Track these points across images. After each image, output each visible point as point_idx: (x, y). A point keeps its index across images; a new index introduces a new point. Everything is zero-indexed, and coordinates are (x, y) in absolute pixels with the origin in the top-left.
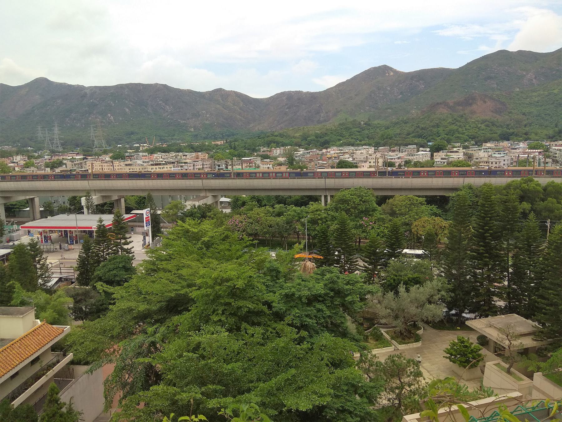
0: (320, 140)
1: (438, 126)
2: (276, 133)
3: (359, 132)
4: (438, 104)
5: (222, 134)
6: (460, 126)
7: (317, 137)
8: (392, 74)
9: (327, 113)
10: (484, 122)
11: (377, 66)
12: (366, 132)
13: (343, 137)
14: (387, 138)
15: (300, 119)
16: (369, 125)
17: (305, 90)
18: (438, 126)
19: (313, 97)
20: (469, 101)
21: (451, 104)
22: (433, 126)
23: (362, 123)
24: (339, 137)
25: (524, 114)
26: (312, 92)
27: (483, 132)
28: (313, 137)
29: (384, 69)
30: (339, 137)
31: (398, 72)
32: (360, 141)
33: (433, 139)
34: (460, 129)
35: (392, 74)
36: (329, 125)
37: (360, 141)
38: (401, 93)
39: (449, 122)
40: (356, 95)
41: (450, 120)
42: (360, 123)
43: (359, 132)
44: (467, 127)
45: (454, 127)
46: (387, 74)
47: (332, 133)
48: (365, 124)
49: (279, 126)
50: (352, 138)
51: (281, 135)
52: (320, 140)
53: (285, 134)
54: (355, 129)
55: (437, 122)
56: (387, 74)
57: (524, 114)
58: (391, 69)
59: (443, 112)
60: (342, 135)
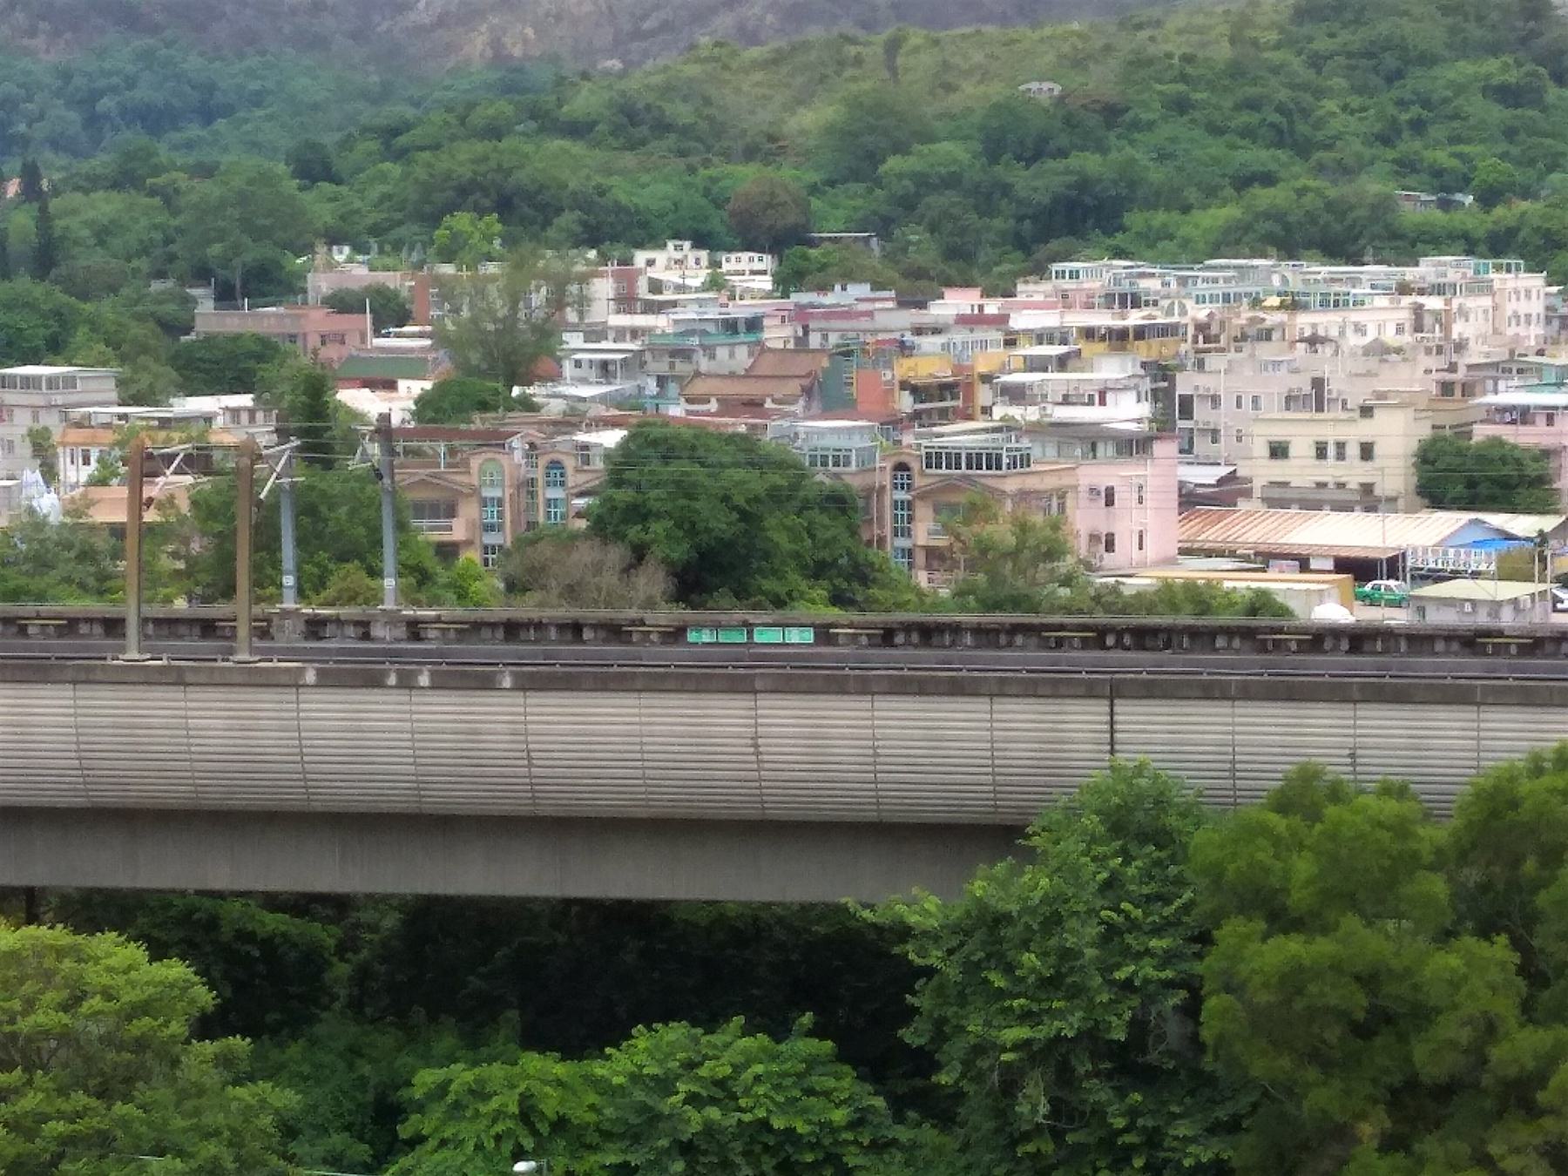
2: (584, 102)
3: (1507, 95)
5: (87, 102)
7: (994, 147)
13: (1303, 149)
24: (1257, 156)
28: (953, 152)
30: (1257, 156)
32: (1489, 198)
37: (1489, 198)
43: (1507, 95)
47: (1181, 106)
51: (634, 124)
53: (682, 112)
54: (1464, 69)
60: (1292, 134)
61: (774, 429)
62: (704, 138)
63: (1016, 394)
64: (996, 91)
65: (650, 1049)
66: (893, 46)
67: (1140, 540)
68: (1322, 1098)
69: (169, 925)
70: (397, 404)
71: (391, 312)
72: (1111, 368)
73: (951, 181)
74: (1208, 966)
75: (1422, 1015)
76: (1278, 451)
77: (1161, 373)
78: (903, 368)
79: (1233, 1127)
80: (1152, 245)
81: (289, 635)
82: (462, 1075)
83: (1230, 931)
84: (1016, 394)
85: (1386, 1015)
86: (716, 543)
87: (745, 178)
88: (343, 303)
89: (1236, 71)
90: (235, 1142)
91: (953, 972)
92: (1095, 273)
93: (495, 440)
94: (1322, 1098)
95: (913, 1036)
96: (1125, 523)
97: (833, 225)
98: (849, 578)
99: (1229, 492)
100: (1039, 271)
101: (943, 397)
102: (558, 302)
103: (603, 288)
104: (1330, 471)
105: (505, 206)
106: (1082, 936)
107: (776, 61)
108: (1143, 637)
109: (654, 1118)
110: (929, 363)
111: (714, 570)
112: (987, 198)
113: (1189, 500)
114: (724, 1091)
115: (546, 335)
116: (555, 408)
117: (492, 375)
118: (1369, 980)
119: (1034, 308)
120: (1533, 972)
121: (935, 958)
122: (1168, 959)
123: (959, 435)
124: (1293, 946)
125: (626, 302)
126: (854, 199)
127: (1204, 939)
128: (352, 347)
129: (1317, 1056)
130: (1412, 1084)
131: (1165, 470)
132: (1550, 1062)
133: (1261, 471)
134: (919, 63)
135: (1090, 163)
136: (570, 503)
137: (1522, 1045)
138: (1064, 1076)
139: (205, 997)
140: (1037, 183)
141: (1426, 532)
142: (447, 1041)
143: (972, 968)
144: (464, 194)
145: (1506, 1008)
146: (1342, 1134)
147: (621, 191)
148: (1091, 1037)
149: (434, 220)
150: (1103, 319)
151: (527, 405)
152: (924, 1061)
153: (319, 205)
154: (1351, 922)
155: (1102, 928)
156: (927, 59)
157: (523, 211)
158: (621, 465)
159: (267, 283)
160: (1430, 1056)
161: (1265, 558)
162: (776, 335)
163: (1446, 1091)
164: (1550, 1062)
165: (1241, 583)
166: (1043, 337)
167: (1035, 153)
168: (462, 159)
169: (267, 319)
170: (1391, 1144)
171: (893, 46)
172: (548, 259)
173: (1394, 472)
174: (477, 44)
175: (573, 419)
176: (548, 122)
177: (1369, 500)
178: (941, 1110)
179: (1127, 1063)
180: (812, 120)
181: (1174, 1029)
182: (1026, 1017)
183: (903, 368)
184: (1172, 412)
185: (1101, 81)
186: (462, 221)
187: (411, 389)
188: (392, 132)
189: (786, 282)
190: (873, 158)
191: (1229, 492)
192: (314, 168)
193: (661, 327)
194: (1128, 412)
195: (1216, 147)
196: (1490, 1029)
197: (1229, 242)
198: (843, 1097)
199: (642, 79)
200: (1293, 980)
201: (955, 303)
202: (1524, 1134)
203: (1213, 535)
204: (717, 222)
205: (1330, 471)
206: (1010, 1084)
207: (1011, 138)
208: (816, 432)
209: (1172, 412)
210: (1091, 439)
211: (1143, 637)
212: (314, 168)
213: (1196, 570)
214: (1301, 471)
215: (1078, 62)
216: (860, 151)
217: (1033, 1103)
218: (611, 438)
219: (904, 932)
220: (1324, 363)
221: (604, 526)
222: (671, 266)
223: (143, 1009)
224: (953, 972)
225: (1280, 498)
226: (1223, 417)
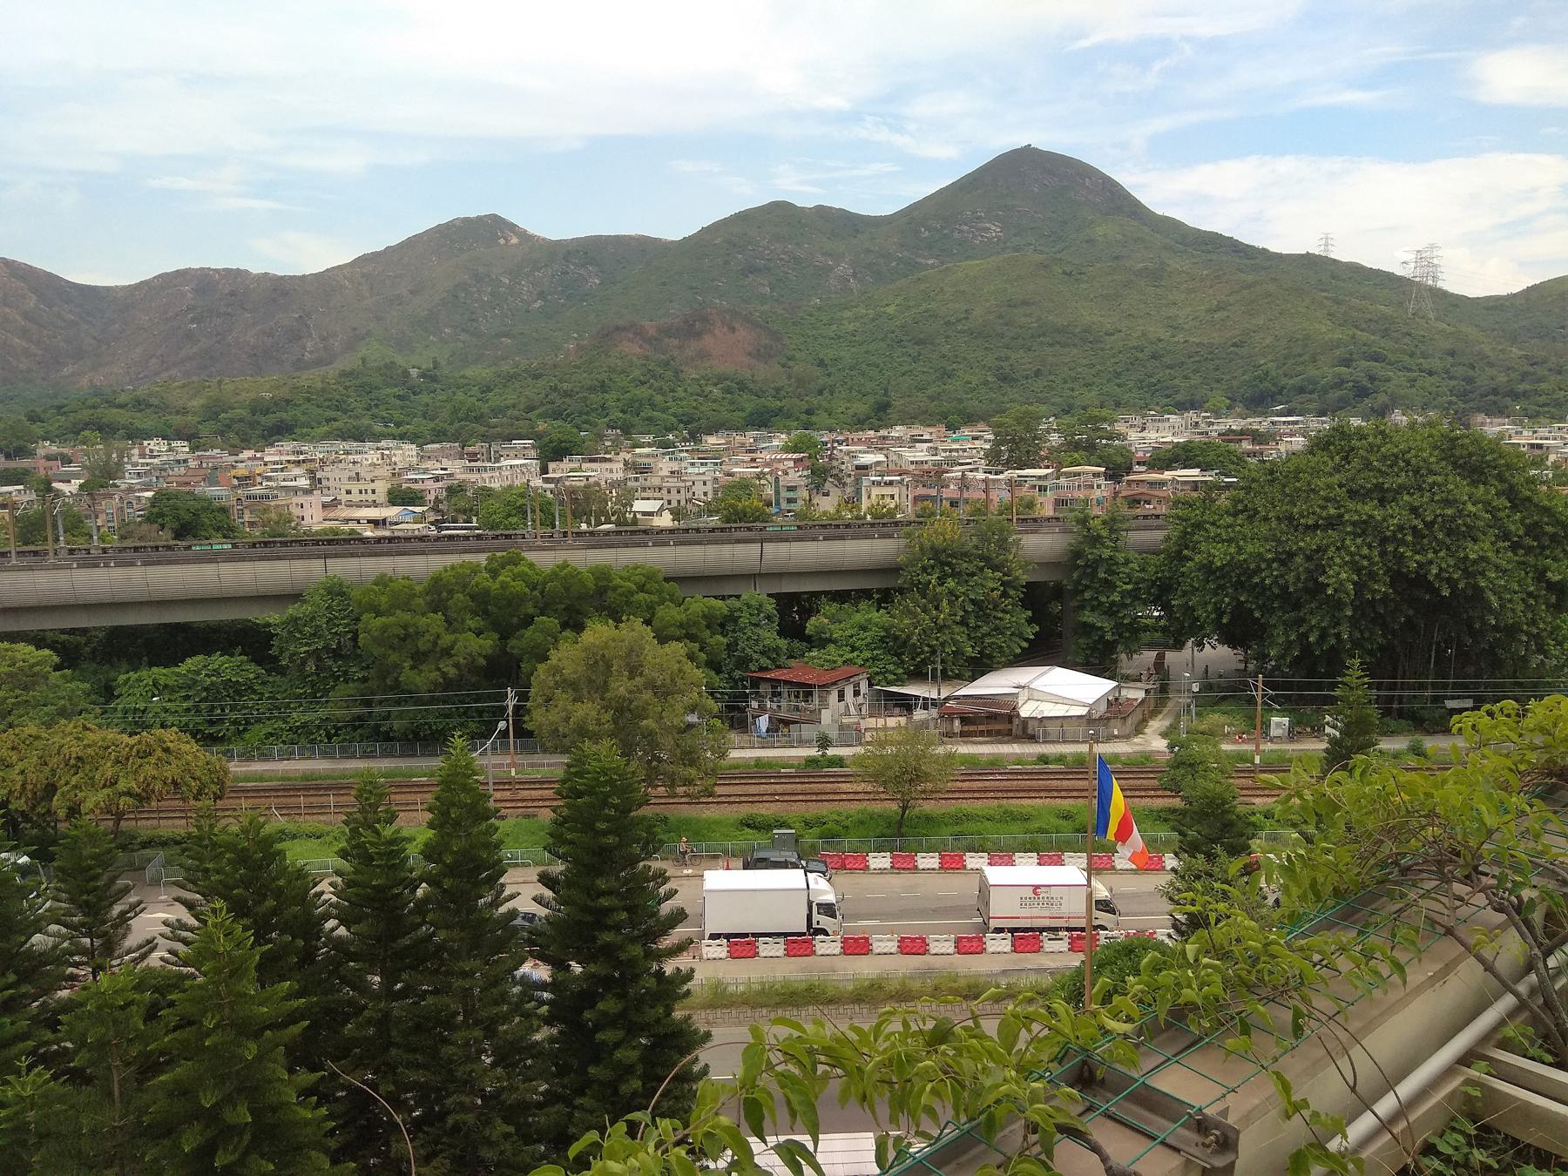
0: (263, 420)
1: (603, 387)
2: (122, 399)
4: (617, 328)
6: (660, 391)
8: (514, 240)
9: (323, 339)
10: (720, 379)
11: (473, 215)
12: (425, 398)
14: (466, 418)
15: (252, 354)
16: (434, 379)
17: (256, 268)
18: (603, 387)
19: (280, 290)
20: (693, 327)
21: (652, 332)
22: (592, 389)
23: (414, 372)
24: (330, 413)
25: (821, 363)
26: (280, 273)
27: (715, 406)
29: (492, 228)
30: (330, 413)
31: (533, 237)
33: (586, 422)
34: (659, 398)
35: (514, 240)
36: (311, 378)
38: (541, 295)
39: (634, 380)
40: (412, 292)
41: (637, 373)
42: (406, 374)
44: (680, 392)
45: (642, 392)
46: (502, 241)
47: (309, 400)
48: (423, 375)
49: (165, 375)
50: (374, 416)
51: (140, 404)
52: (263, 420)
53: (153, 401)
55: (604, 376)
56: (502, 241)
57: (821, 363)
58: (512, 227)
59: (631, 349)
61: (198, 490)
62: (162, 408)
63: (269, 479)
64: (253, 395)
66: (219, 382)
67: (313, 517)
69: (39, 641)
70: (72, 487)
71: (67, 460)
72: (297, 471)
73: (241, 420)
76: (348, 492)
77: (312, 472)
78: (233, 472)
79: (368, 667)
80: (303, 438)
81: (63, 554)
84: (269, 479)
86: (184, 523)
87: (177, 420)
88: (48, 458)
89: (323, 390)
91: (285, 634)
92: (288, 446)
93: (111, 496)
95: (274, 652)
96: (307, 513)
97: (205, 430)
98: (228, 531)
99: (335, 503)
100: (272, 445)
101: (246, 480)
102: (121, 457)
103: (136, 451)
104: (363, 497)
105: (100, 429)
107: (184, 386)
108: (316, 542)
110: (242, 470)
111: (186, 530)
112: (253, 425)
113: (324, 506)
115: (120, 464)
116: (123, 487)
117: (101, 479)
119: (271, 455)
121: (279, 631)
123: (256, 490)
125: (142, 456)
126: (211, 426)
128: (55, 470)
131: (318, 498)
133: (344, 497)
134: (228, 387)
135: (284, 415)
136: (135, 514)
138: (319, 659)
139: (56, 659)
140: (268, 420)
141: (392, 512)
143: (290, 632)
144: (86, 426)
147: (137, 423)
148: (326, 648)
149: (78, 433)
150: (292, 458)
151: (115, 485)
153: (37, 429)
156: (231, 387)
157: (107, 430)
158: (154, 502)
159: (21, 452)
161: (347, 521)
162: (192, 464)
165: (346, 528)
166: (275, 463)
167: (266, 412)
168: (85, 415)
169: (25, 463)
170: (412, 668)
171: (219, 382)
172: (116, 444)
173: (381, 496)
174: (85, 381)
175: (130, 489)
176: (111, 404)
177: (375, 504)
179: (336, 654)
180: (196, 403)
181: (349, 644)
182: (307, 644)
183: (233, 472)
184: (316, 482)
185: (284, 393)
186: (86, 433)
187: (76, 483)
188: (59, 408)
189: (193, 449)
190: (217, 414)
191: (335, 503)
192: (34, 418)
193: (153, 466)
194: (304, 482)
195: (320, 411)
197: (326, 437)
199: (142, 392)
201: (247, 454)
203: (332, 515)
204: (169, 432)
205: (363, 497)
206: (304, 662)
207: (258, 408)
208: (214, 491)
209: (316, 482)
210: (296, 490)
211: (316, 542)
212: (34, 418)
213: (328, 524)
214: (355, 497)
215: (278, 388)
216: (213, 412)
217: (311, 667)
218: (149, 494)
219: (269, 625)
220: (358, 468)
221: (149, 519)
222: (154, 445)
223: (37, 664)
224: (285, 634)
225: (350, 505)
226: (330, 484)
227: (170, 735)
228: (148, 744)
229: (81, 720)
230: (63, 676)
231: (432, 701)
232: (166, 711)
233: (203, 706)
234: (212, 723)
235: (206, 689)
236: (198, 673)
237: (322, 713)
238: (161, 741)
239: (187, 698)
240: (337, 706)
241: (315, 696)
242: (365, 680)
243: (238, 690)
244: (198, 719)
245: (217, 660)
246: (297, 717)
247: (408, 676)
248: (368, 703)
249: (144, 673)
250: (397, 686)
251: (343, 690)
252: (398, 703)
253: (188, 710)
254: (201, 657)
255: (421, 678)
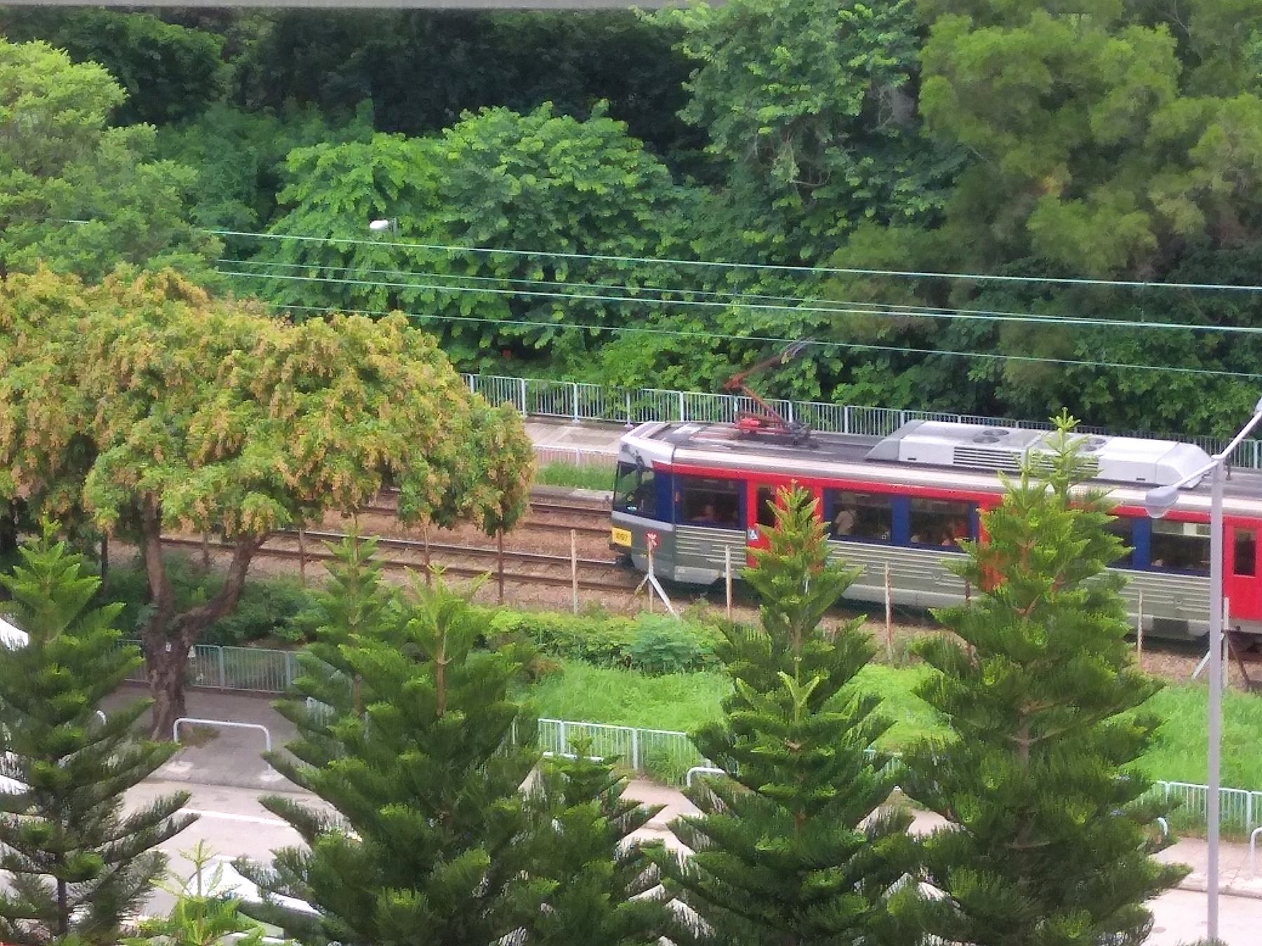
65: (477, 130)
68: (1015, 158)
74: (928, 53)
75: (1098, 90)
79: (946, 183)
82: (327, 153)
83: (943, 26)
85: (1067, 91)
90: (147, 208)
91: (720, 64)
94: (1015, 158)
95: (688, 116)
106: (824, 32)
109: (480, 185)
114: (538, 163)
118: (1055, 63)
120: (1187, 54)
121: (705, 52)
122: (893, 49)
124: (992, 37)
127: (922, 32)
129: (1014, 125)
130: (1089, 146)
132: (1200, 125)
137: (1177, 113)
138: (810, 145)
142: (315, 124)
143: (736, 61)
145: (1166, 84)
146: (1032, 187)
148: (833, 114)
152: (699, 136)
154: (1040, 16)
155: (840, 25)
160: (1103, 122)
163: (1114, 153)
164: (1200, 125)
170: (1072, 193)
178: (714, 176)
179: (861, 133)
181: (898, 106)
182: (780, 99)
196: (1153, 100)
198: (633, 165)
200: (994, 64)
202: (1180, 184)
206: (767, 154)
217: (786, 168)
219: (679, 33)
224: (720, 64)
227: (381, 335)
228: (321, 353)
229: (164, 266)
230: (133, 144)
231: (1122, 304)
232: (404, 261)
233: (500, 255)
234: (519, 308)
235: (509, 209)
236: (490, 159)
237: (811, 309)
238: (356, 346)
239: (458, 230)
240: (844, 298)
241: (792, 260)
242: (934, 220)
243: (592, 219)
244: (487, 293)
245: (544, 127)
246: (742, 313)
247: (1055, 219)
248: (938, 294)
249: (353, 150)
250: (1016, 251)
251: (867, 248)
252: (1025, 299)
253: (459, 264)
254: (497, 116)
255: (1095, 230)
